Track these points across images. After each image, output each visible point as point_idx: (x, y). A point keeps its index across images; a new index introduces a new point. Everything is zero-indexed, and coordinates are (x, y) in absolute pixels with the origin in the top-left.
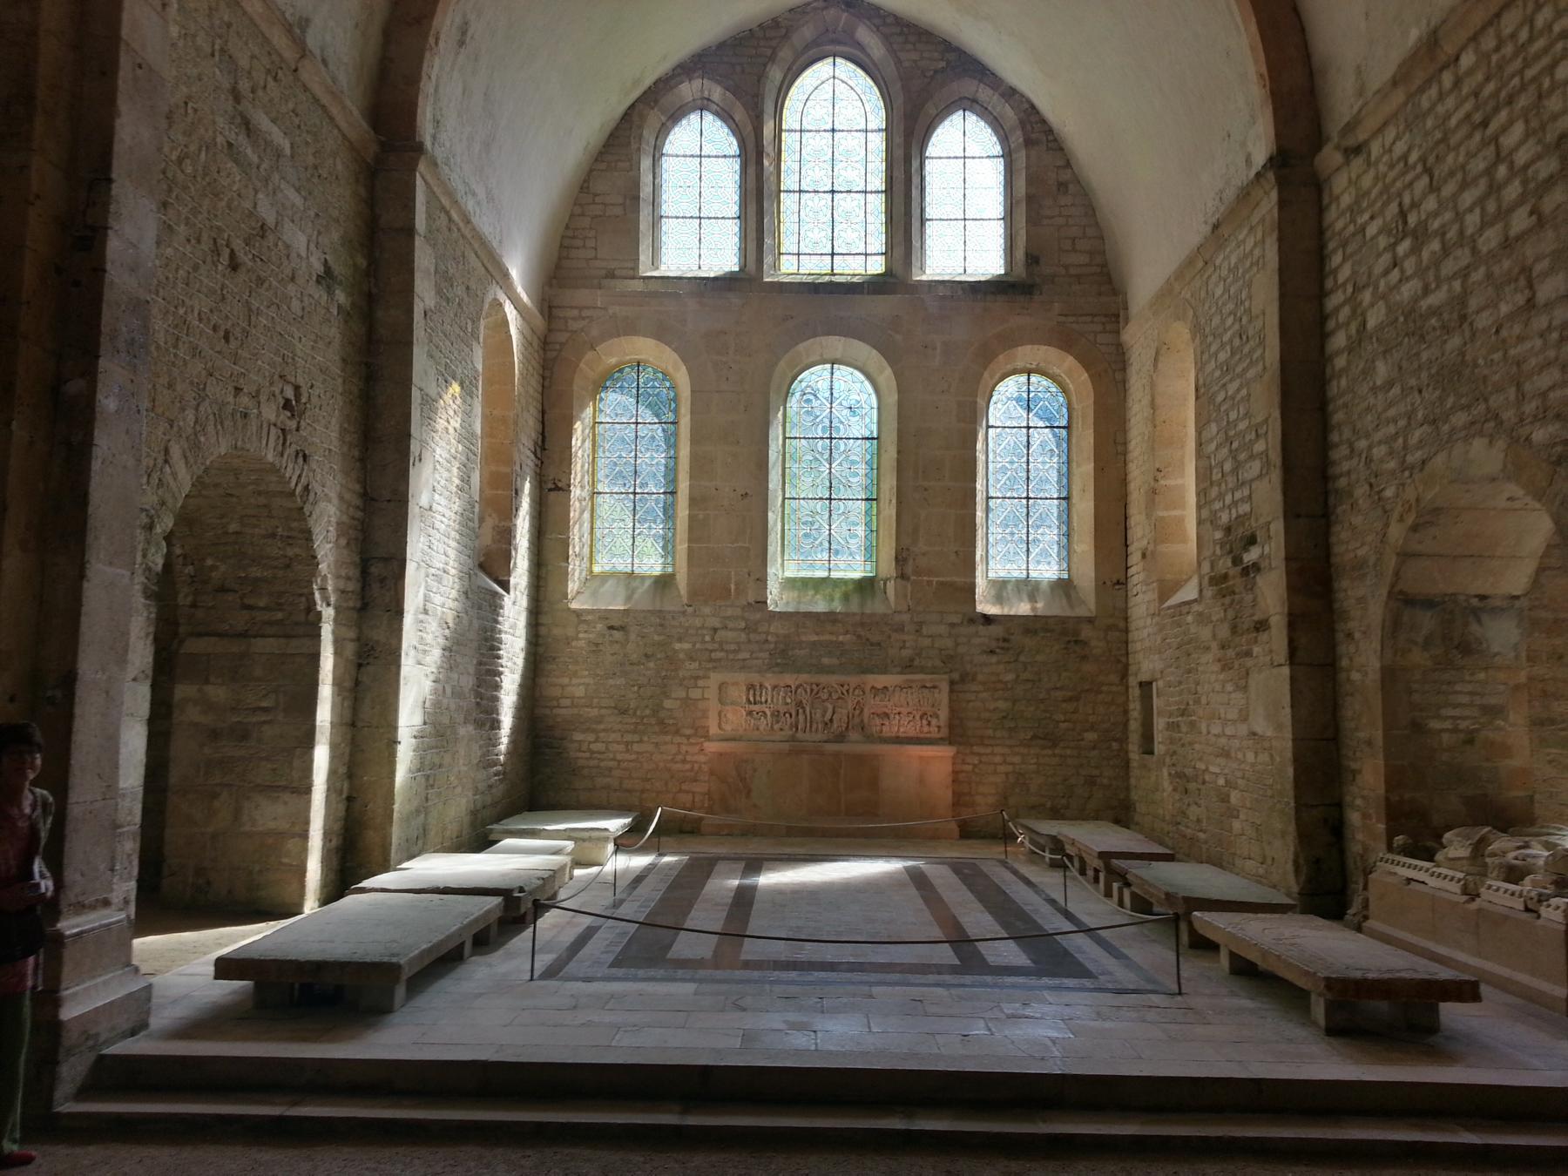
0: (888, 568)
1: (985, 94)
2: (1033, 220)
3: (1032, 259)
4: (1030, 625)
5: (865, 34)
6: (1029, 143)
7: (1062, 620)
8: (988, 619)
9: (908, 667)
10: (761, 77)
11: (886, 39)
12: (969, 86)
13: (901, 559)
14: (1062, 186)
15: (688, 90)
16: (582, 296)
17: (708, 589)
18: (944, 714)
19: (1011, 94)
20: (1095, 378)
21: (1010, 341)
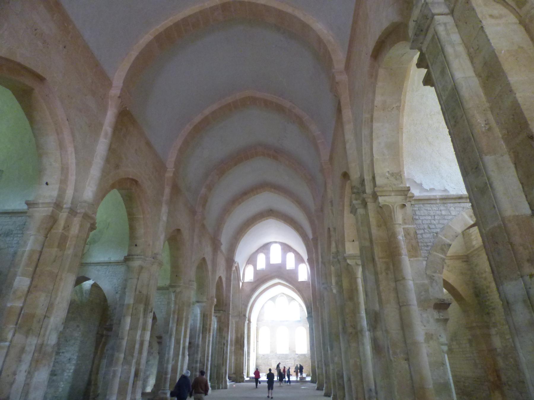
4: (302, 355)
9: (290, 359)
17: (272, 352)
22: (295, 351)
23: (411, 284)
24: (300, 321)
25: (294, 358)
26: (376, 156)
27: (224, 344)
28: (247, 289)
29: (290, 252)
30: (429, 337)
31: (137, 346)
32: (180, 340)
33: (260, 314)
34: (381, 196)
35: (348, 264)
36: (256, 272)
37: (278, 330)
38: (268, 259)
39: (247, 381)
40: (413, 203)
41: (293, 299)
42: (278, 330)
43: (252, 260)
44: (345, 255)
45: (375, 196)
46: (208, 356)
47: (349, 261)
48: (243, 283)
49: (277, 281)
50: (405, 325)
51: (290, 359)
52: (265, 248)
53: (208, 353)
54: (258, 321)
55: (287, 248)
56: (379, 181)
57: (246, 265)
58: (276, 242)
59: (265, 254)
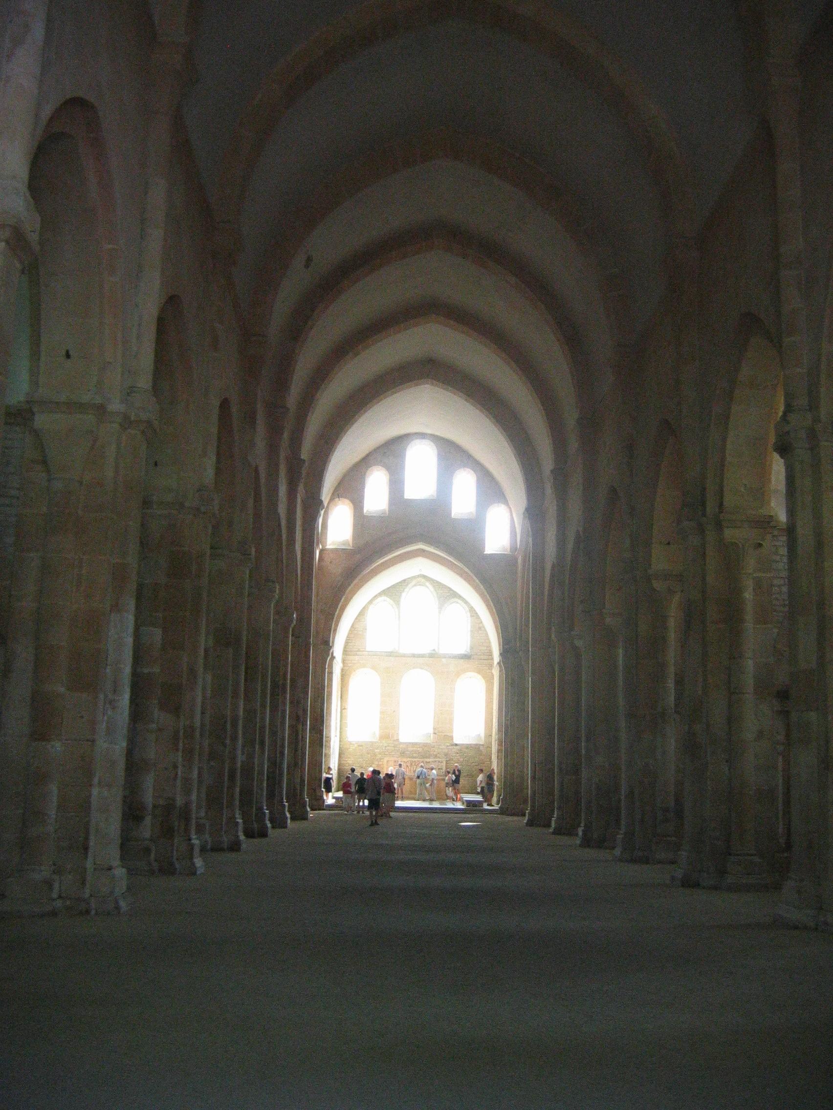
0: (431, 731)
1: (459, 601)
2: (472, 637)
3: (472, 648)
5: (427, 584)
6: (471, 616)
7: (476, 745)
8: (456, 745)
9: (436, 756)
10: (400, 597)
11: (434, 586)
12: (456, 600)
13: (434, 729)
14: (480, 628)
15: (380, 599)
16: (351, 658)
17: (385, 736)
18: (444, 768)
19: (466, 602)
20: (487, 682)
21: (464, 671)
22: (452, 738)
23: (749, 665)
24: (466, 657)
25: (446, 755)
26: (729, 459)
27: (298, 718)
28: (335, 569)
29: (465, 466)
30: (760, 735)
31: (229, 726)
32: (255, 710)
33: (354, 633)
34: (728, 527)
35: (654, 590)
36: (361, 520)
37: (415, 679)
38: (396, 485)
39: (331, 807)
40: (776, 533)
41: (454, 595)
42: (415, 679)
43: (351, 487)
44: (650, 572)
45: (719, 526)
46: (283, 746)
47: (656, 584)
48: (321, 551)
49: (421, 546)
50: (732, 720)
51: (436, 756)
52: (390, 452)
53: (283, 739)
54: (346, 652)
55: (452, 454)
56: (729, 500)
57: (332, 500)
58: (422, 436)
59: (388, 468)
